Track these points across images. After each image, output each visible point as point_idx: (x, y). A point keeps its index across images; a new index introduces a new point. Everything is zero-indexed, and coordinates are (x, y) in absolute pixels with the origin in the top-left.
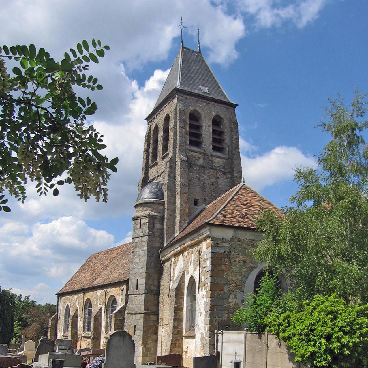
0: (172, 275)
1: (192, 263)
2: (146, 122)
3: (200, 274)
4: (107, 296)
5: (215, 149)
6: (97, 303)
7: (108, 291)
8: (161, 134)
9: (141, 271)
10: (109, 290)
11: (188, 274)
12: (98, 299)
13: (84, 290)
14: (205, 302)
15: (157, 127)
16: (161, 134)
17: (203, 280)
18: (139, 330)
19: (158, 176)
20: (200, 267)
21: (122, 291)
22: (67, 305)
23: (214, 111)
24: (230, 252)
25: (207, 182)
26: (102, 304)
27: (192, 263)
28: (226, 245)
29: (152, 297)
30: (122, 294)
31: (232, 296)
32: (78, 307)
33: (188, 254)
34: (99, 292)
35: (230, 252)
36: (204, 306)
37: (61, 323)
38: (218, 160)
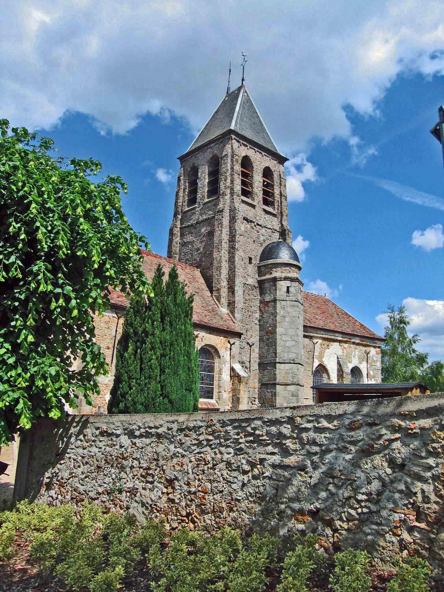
19: (258, 224)
30: (231, 349)
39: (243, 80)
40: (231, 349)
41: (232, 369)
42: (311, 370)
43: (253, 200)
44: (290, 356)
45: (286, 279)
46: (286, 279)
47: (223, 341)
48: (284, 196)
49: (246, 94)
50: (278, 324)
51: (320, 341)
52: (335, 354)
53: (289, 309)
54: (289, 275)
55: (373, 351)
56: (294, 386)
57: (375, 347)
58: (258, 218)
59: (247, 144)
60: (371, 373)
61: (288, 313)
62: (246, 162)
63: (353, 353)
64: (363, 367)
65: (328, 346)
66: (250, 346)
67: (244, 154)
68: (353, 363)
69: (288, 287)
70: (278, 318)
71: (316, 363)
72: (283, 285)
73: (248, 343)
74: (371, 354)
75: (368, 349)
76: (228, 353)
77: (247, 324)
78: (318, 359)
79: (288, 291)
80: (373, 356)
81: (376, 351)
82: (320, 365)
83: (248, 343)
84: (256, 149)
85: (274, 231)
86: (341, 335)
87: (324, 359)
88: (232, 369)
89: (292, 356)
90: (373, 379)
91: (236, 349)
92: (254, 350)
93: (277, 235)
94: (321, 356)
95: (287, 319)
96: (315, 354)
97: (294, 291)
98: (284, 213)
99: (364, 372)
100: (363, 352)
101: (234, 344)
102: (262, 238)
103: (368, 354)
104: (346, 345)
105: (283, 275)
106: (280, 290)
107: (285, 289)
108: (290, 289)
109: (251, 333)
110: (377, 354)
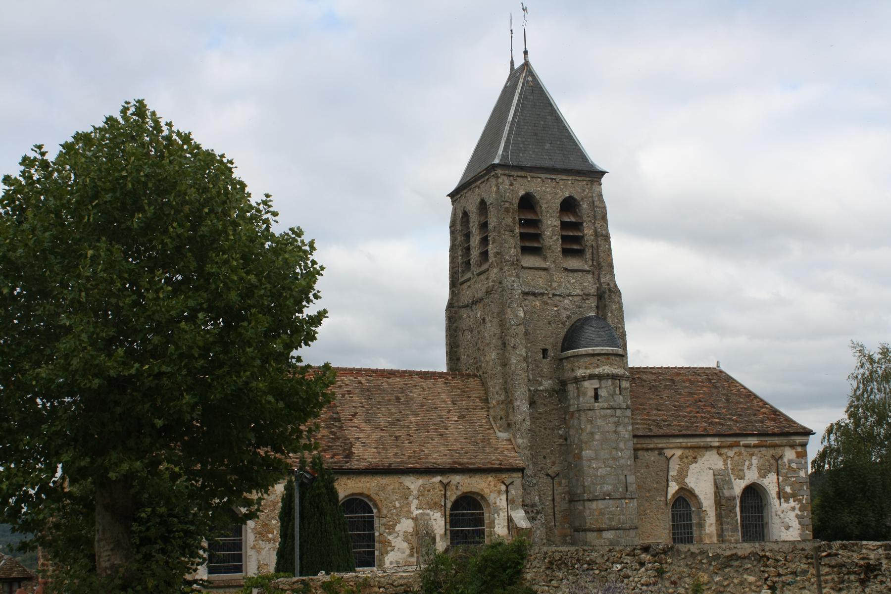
0: (673, 473)
1: (754, 468)
4: (448, 493)
7: (454, 482)
9: (629, 463)
10: (456, 479)
11: (742, 478)
12: (411, 498)
14: (797, 516)
19: (554, 295)
20: (778, 475)
21: (507, 487)
26: (430, 508)
27: (754, 468)
30: (507, 492)
34: (414, 484)
39: (526, 53)
40: (507, 492)
41: (510, 520)
42: (663, 499)
43: (545, 259)
44: (605, 489)
45: (591, 377)
46: (591, 377)
47: (492, 483)
48: (602, 235)
49: (530, 79)
50: (584, 445)
51: (679, 453)
52: (710, 469)
53: (599, 422)
54: (596, 371)
56: (613, 532)
57: (792, 446)
58: (555, 285)
59: (528, 174)
60: (788, 489)
61: (599, 427)
62: (528, 203)
63: (747, 463)
64: (770, 483)
65: (695, 458)
66: (553, 478)
67: (522, 193)
68: (746, 478)
69: (596, 389)
70: (584, 437)
71: (673, 488)
72: (589, 386)
73: (548, 475)
74: (786, 460)
75: (779, 451)
76: (504, 497)
77: (544, 448)
78: (676, 481)
79: (596, 397)
80: (790, 462)
81: (797, 453)
82: (681, 489)
83: (548, 475)
84: (543, 176)
85: (585, 297)
86: (717, 439)
87: (687, 480)
88: (510, 520)
89: (608, 488)
90: (791, 500)
92: (560, 484)
93: (593, 302)
94: (682, 475)
95: (597, 437)
96: (671, 473)
97: (606, 394)
98: (603, 264)
100: (768, 457)
101: (512, 483)
102: (564, 314)
103: (778, 459)
104: (731, 453)
105: (588, 372)
106: (585, 394)
107: (592, 393)
108: (600, 392)
109: (553, 459)
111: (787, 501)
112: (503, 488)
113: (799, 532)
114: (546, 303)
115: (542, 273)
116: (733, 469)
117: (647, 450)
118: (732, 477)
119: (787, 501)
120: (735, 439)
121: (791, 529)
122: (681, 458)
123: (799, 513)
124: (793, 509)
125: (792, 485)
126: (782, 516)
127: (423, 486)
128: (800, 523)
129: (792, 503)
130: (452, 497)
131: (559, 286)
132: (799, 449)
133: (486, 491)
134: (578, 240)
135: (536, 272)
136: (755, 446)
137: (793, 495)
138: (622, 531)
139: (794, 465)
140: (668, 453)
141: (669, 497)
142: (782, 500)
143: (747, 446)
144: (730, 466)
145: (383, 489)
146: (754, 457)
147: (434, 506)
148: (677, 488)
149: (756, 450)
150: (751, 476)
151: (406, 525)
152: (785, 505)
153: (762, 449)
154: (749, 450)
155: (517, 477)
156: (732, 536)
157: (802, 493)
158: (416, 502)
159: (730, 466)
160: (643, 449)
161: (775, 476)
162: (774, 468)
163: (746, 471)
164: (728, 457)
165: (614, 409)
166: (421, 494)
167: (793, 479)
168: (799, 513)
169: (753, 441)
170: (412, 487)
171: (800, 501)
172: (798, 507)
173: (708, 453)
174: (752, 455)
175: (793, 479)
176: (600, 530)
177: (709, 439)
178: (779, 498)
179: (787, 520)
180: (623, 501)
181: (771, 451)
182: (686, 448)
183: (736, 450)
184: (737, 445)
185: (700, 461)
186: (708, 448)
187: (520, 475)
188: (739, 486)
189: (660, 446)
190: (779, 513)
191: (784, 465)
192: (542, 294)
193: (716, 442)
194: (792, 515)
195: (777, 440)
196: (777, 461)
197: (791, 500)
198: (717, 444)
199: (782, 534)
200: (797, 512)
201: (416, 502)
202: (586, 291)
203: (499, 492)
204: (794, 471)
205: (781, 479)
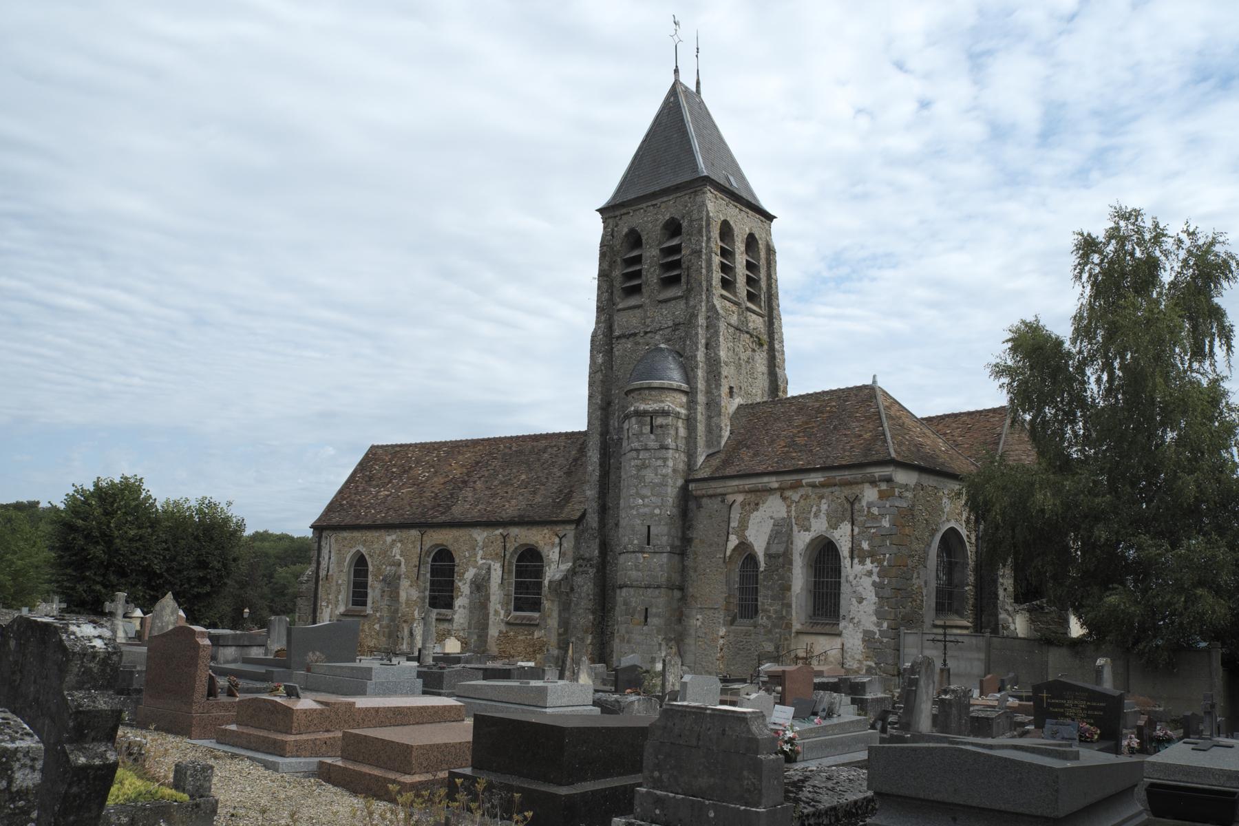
0: (734, 524)
2: (599, 216)
3: (853, 536)
4: (508, 545)
5: (751, 297)
6: (475, 555)
8: (651, 253)
9: (657, 511)
10: (514, 531)
11: (808, 530)
13: (424, 526)
14: (874, 584)
15: (635, 239)
16: (651, 253)
17: (865, 546)
18: (656, 615)
19: (646, 333)
20: (853, 524)
22: (354, 550)
23: (743, 224)
24: (913, 506)
25: (744, 356)
28: (909, 495)
29: (677, 558)
30: (561, 544)
31: (915, 575)
32: (398, 557)
33: (806, 497)
34: (480, 535)
35: (913, 506)
36: (872, 588)
37: (334, 588)
38: (754, 316)
40: (561, 544)
51: (740, 498)
55: (870, 494)
57: (873, 482)
58: (648, 321)
60: (865, 546)
63: (814, 509)
64: (842, 537)
65: (757, 504)
71: (733, 541)
74: (864, 503)
86: (774, 479)
90: (868, 561)
91: (568, 544)
94: (743, 525)
96: (732, 525)
99: (844, 548)
103: (853, 501)
104: (796, 497)
110: (881, 498)
111: (862, 562)
112: (557, 540)
113: (874, 607)
114: (637, 344)
115: (637, 311)
116: (797, 518)
117: (710, 496)
118: (795, 528)
119: (862, 562)
120: (795, 477)
121: (865, 602)
122: (743, 505)
123: (877, 580)
124: (870, 573)
125: (871, 539)
126: (854, 582)
127: (488, 537)
128: (877, 595)
129: (869, 565)
130: (511, 547)
131: (652, 322)
132: (884, 486)
133: (541, 543)
134: (677, 264)
135: (631, 312)
136: (823, 485)
137: (872, 554)
138: (632, 590)
139: (875, 511)
140: (730, 498)
141: (728, 553)
142: (856, 561)
143: (813, 486)
144: (793, 513)
145: (456, 540)
146: (824, 501)
147: (496, 557)
148: (737, 542)
149: (826, 491)
150: (819, 526)
151: (470, 574)
152: (858, 568)
153: (833, 489)
154: (817, 490)
155: (570, 530)
156: (771, 605)
157: (883, 550)
158: (481, 553)
159: (793, 513)
160: (703, 496)
161: (849, 526)
162: (848, 514)
163: (813, 520)
164: (793, 502)
165: (636, 450)
166: (485, 546)
167: (873, 531)
168: (877, 580)
169: (817, 478)
170: (479, 539)
171: (880, 563)
172: (876, 570)
173: (771, 498)
174: (822, 497)
175: (873, 531)
176: (621, 587)
177: (766, 479)
178: (852, 558)
179: (860, 589)
180: (640, 555)
181: (847, 491)
182: (750, 491)
183: (802, 491)
184: (796, 486)
185: (762, 508)
186: (771, 491)
187: (573, 527)
188: (802, 540)
189: (719, 491)
190: (851, 578)
191: (861, 510)
192: (635, 335)
193: (774, 482)
194: (867, 582)
195: (847, 475)
196: (852, 504)
197: (868, 561)
198: (776, 485)
199: (852, 608)
200: (875, 578)
201: (481, 553)
202: (677, 321)
203: (553, 545)
204: (875, 518)
205: (856, 530)
